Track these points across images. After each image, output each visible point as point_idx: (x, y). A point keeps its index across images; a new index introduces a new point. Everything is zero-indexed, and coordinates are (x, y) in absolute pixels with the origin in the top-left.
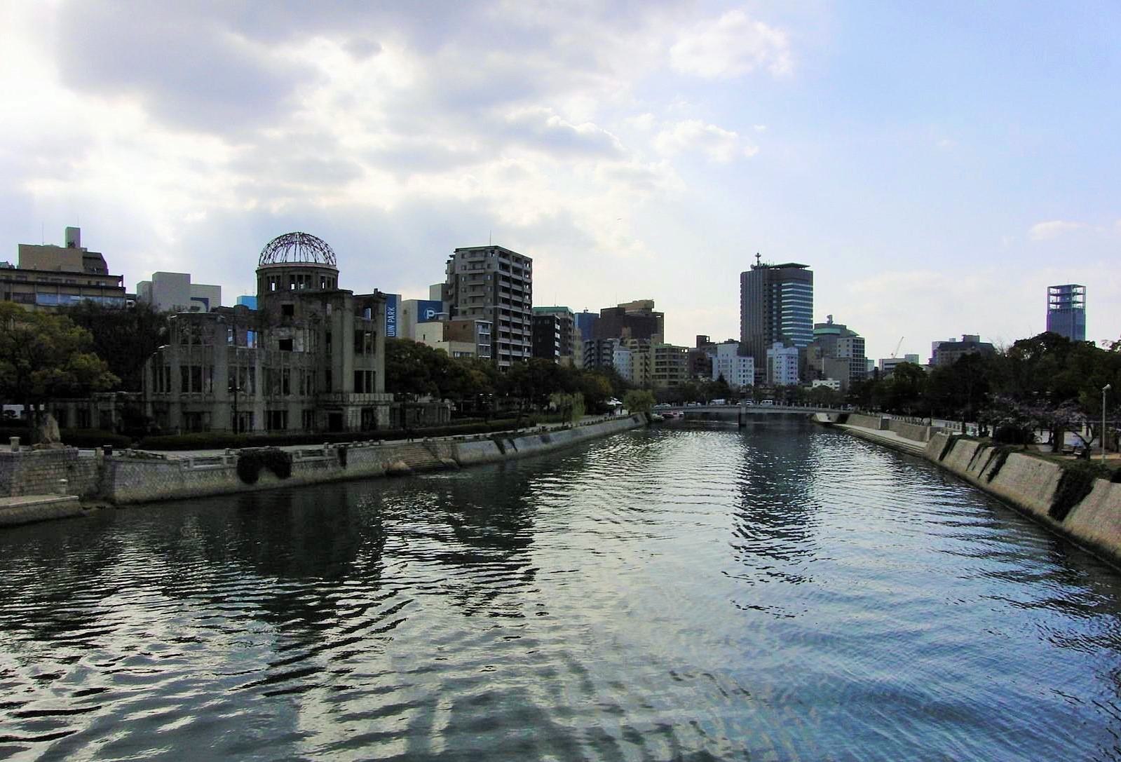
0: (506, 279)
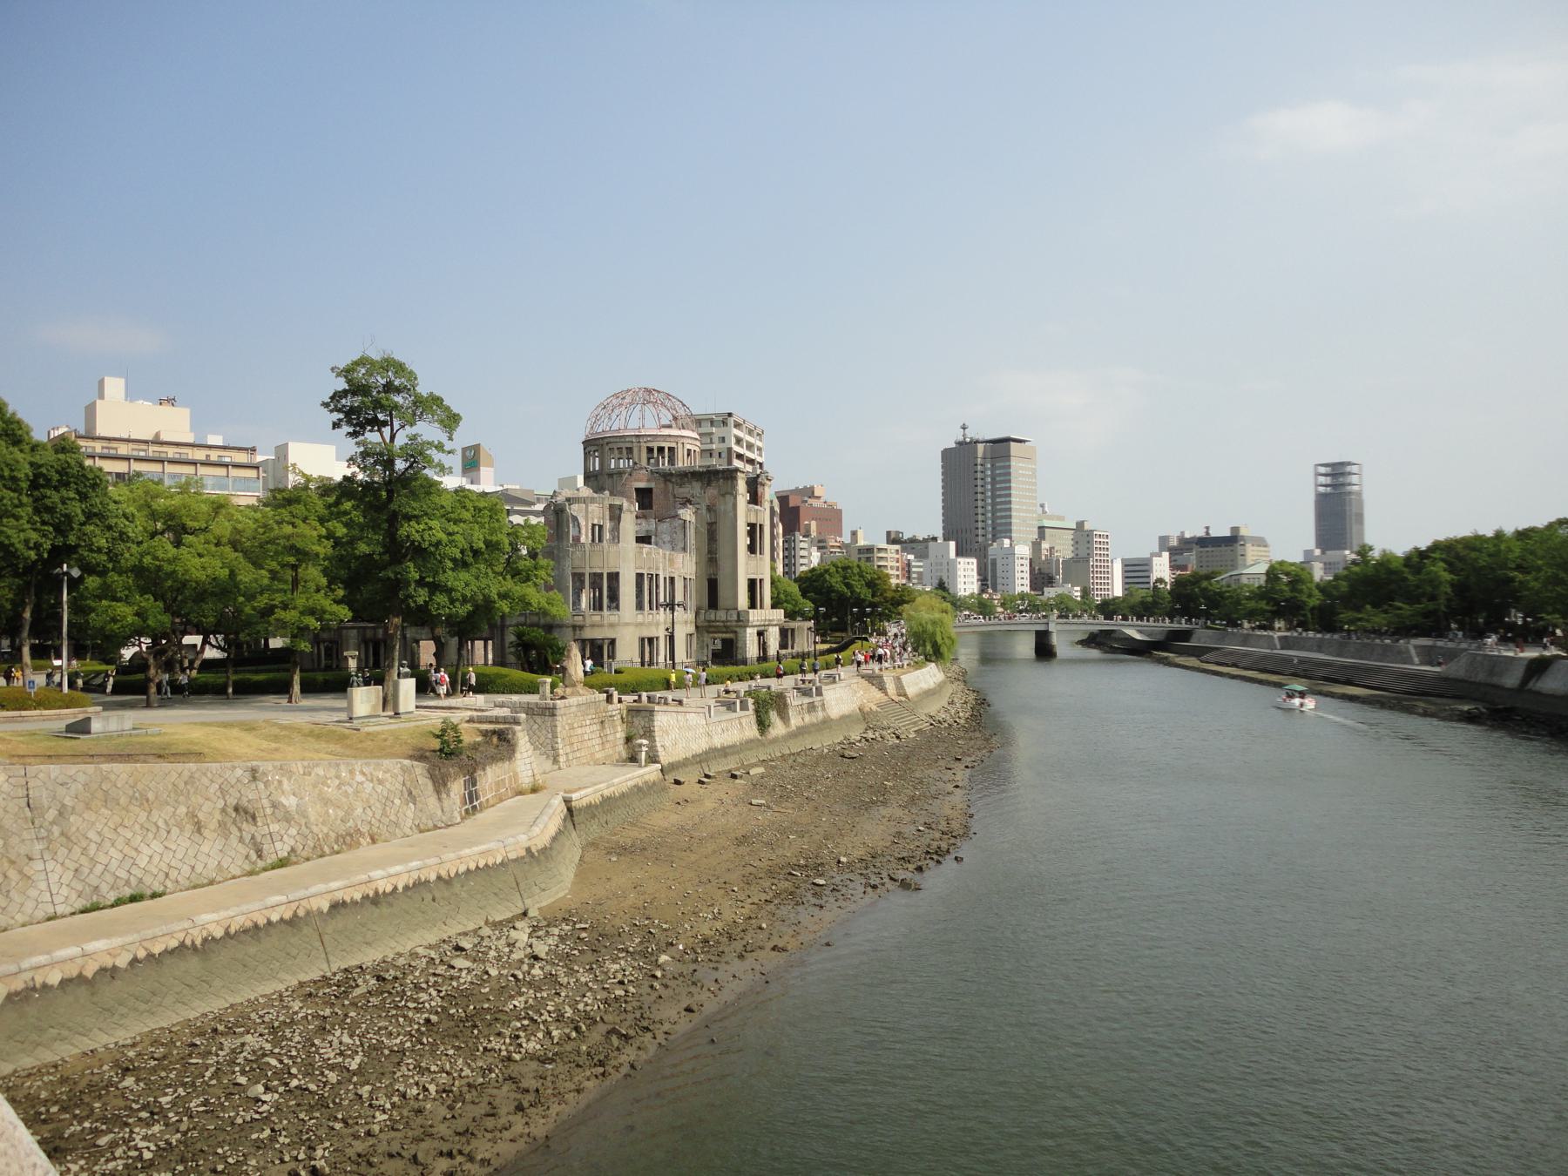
0: (740, 457)
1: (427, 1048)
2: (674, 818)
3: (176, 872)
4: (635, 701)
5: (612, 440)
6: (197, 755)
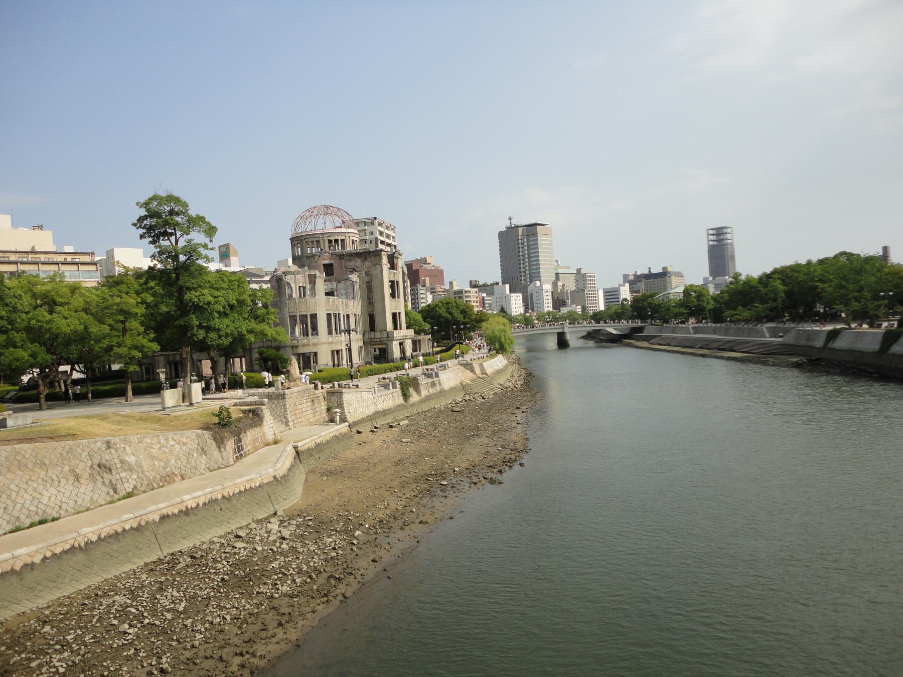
0: (382, 242)
1: (223, 595)
2: (358, 453)
3: (66, 505)
4: (331, 387)
5: (307, 237)
6: (73, 436)
